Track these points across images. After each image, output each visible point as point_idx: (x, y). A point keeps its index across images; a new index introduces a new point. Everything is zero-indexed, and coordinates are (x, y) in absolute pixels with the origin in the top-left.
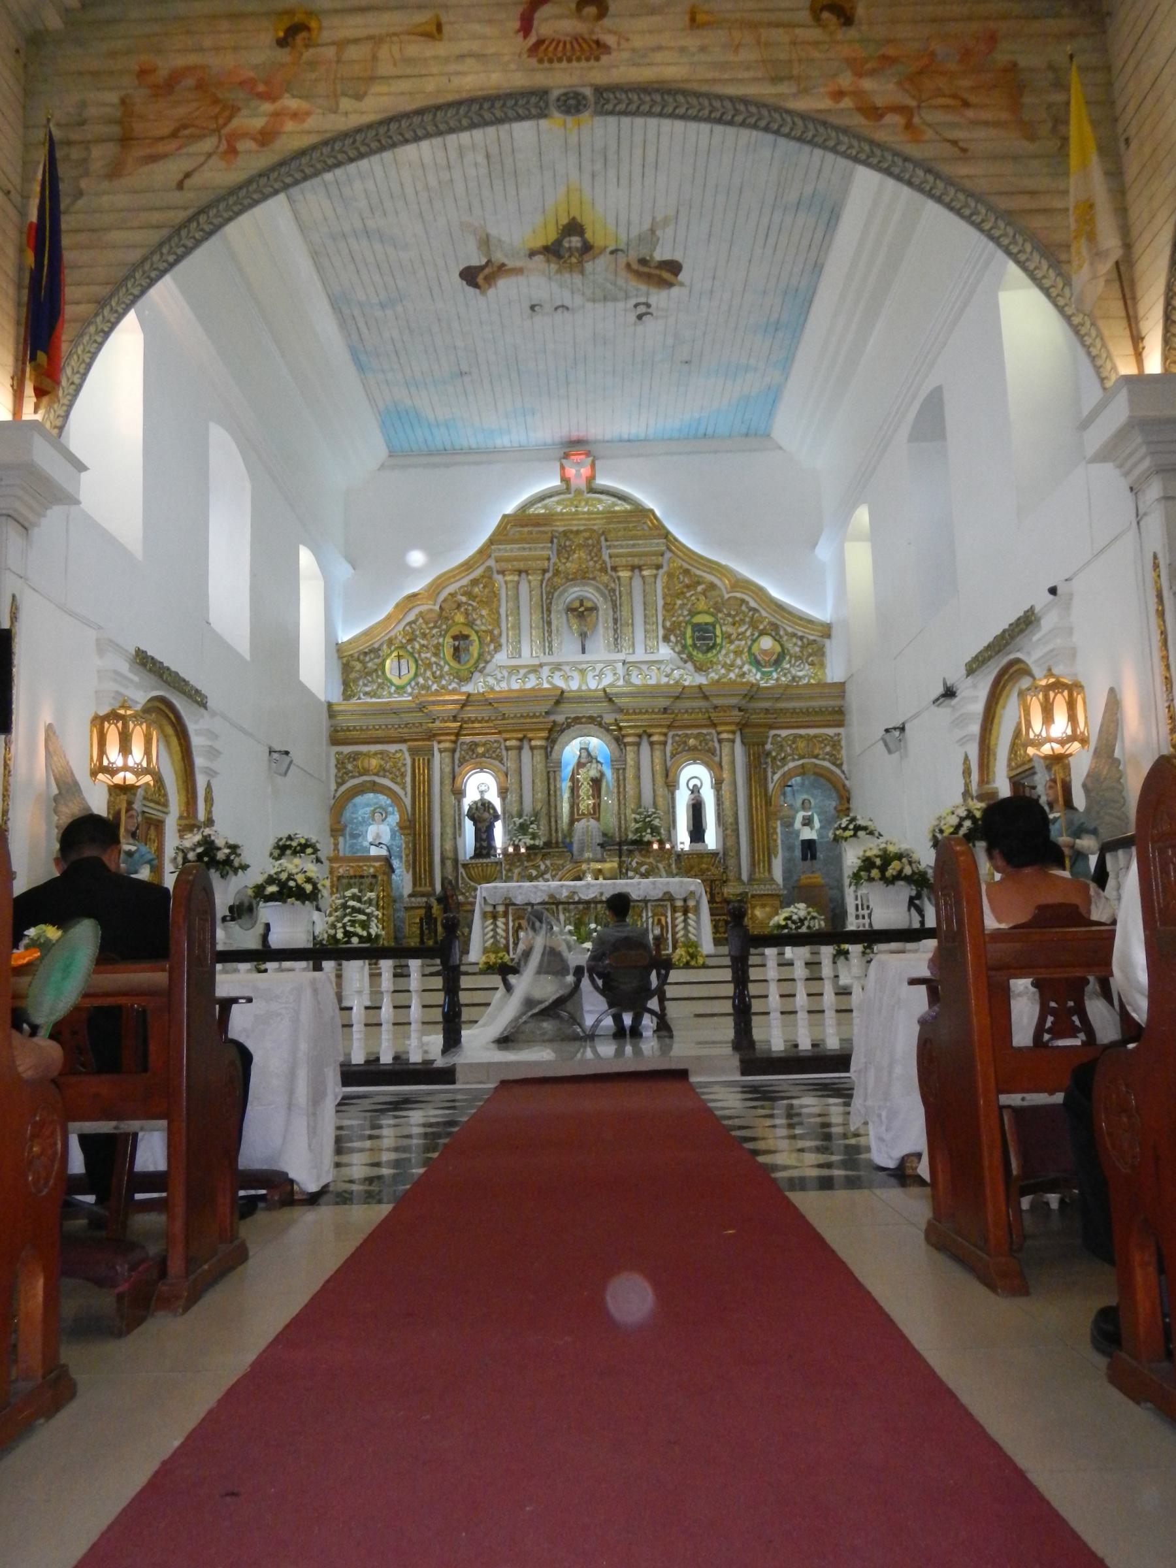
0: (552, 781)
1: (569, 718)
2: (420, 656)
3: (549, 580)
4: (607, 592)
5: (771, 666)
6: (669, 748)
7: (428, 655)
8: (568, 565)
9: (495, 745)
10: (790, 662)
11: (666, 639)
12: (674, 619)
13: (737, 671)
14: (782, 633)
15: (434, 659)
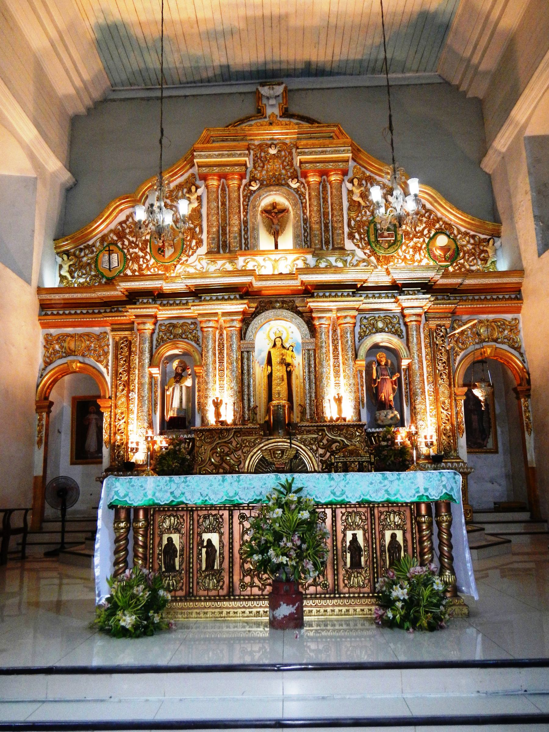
0: (245, 361)
1: (263, 302)
2: (128, 251)
3: (246, 185)
4: (297, 196)
5: (446, 261)
6: (357, 329)
7: (137, 250)
8: (264, 172)
9: (192, 326)
10: (463, 257)
11: (351, 236)
12: (358, 219)
13: (416, 264)
14: (455, 232)
15: (141, 254)
